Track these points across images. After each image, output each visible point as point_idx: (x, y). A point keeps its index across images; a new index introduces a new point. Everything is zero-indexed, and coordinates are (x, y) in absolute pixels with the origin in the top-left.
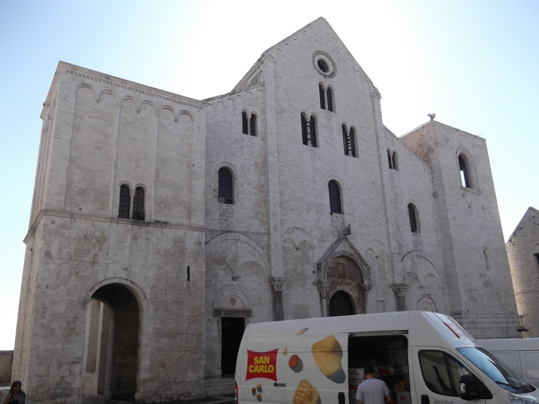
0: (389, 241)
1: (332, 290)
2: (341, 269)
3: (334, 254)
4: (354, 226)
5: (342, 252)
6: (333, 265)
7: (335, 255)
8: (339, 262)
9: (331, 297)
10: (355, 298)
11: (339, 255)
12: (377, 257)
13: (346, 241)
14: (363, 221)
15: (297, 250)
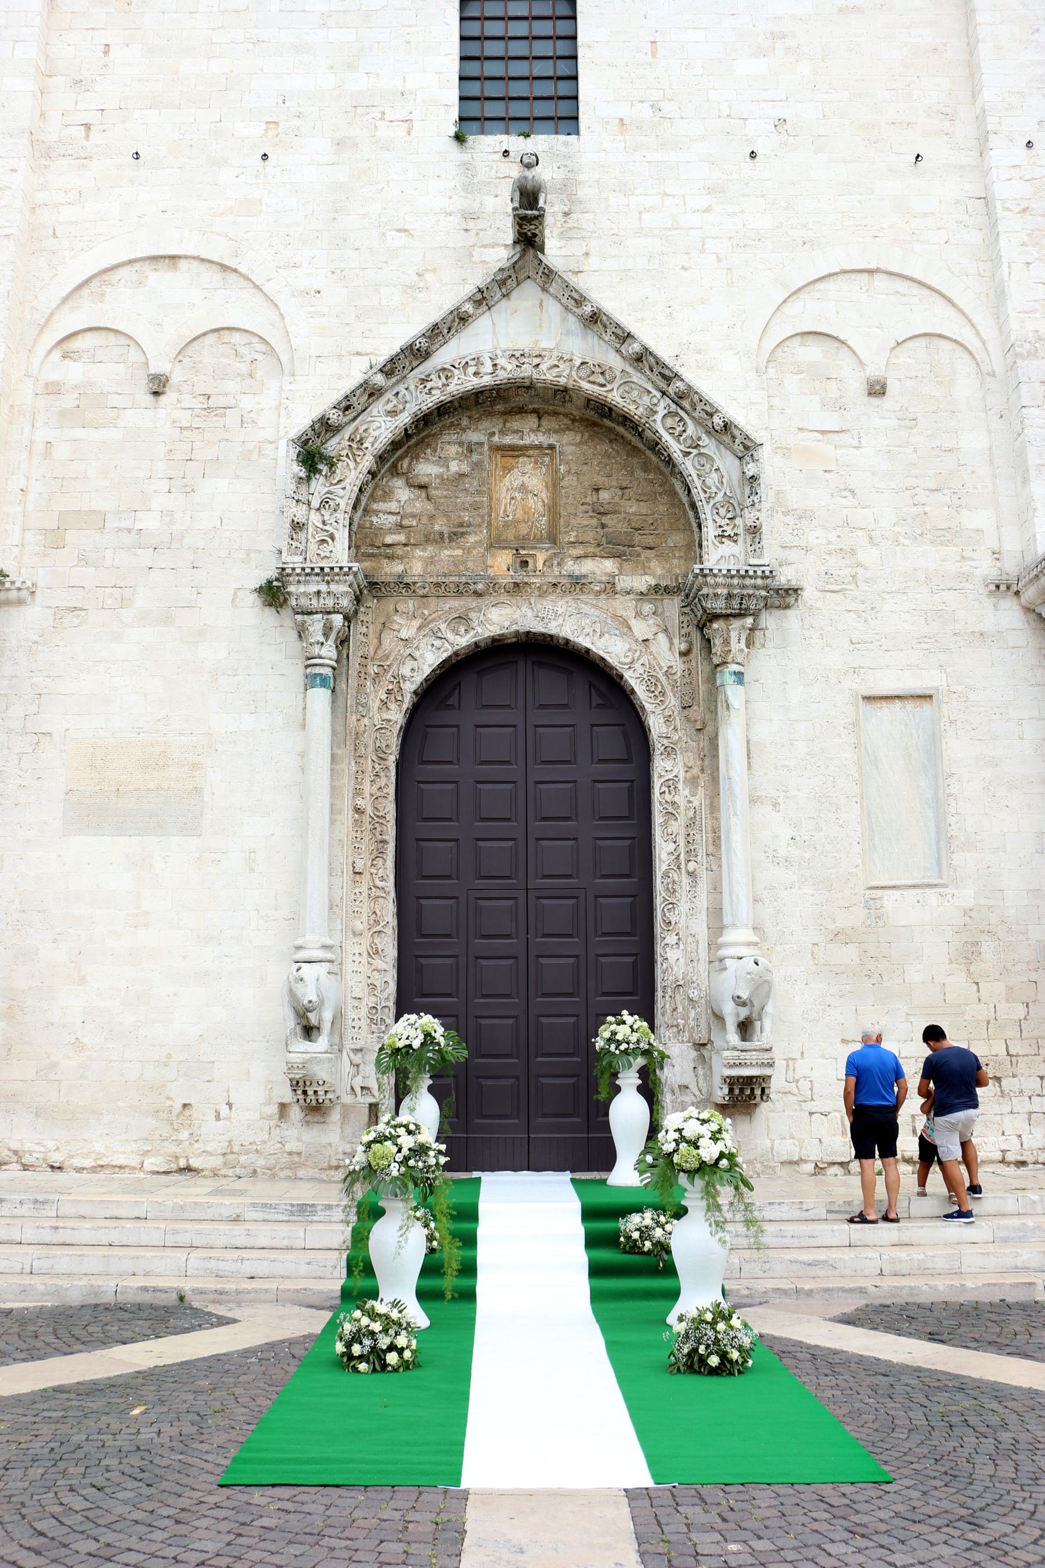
0: (995, 261)
1: (436, 634)
2: (523, 488)
3: (423, 381)
4: (665, 194)
5: (502, 361)
6: (454, 467)
7: (436, 382)
8: (509, 440)
9: (419, 678)
10: (652, 682)
11: (472, 383)
12: (877, 390)
13: (544, 289)
14: (753, 155)
15: (156, 394)
